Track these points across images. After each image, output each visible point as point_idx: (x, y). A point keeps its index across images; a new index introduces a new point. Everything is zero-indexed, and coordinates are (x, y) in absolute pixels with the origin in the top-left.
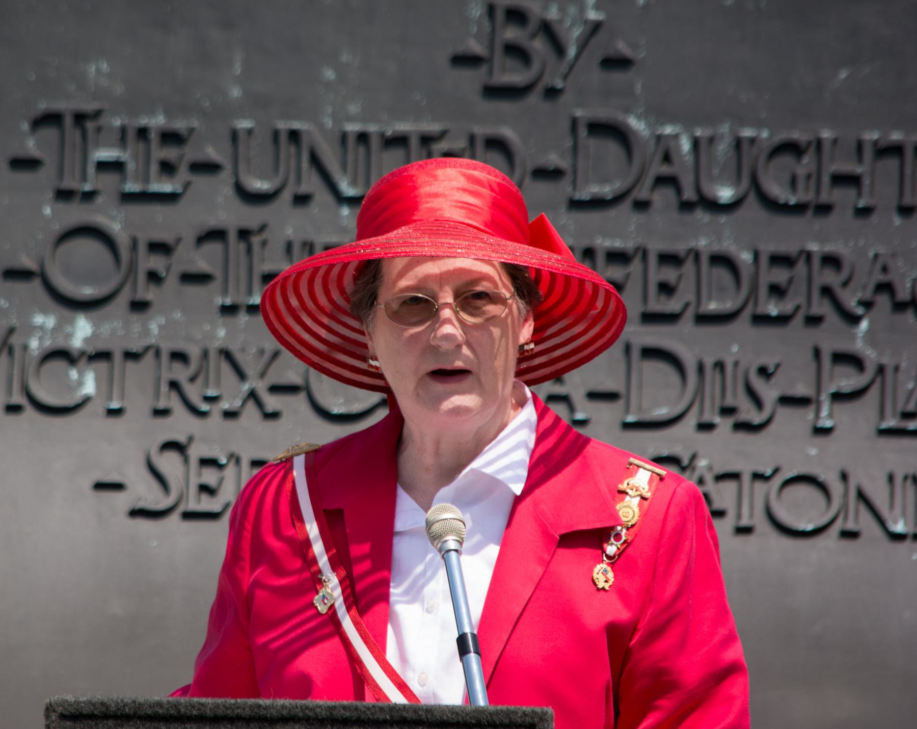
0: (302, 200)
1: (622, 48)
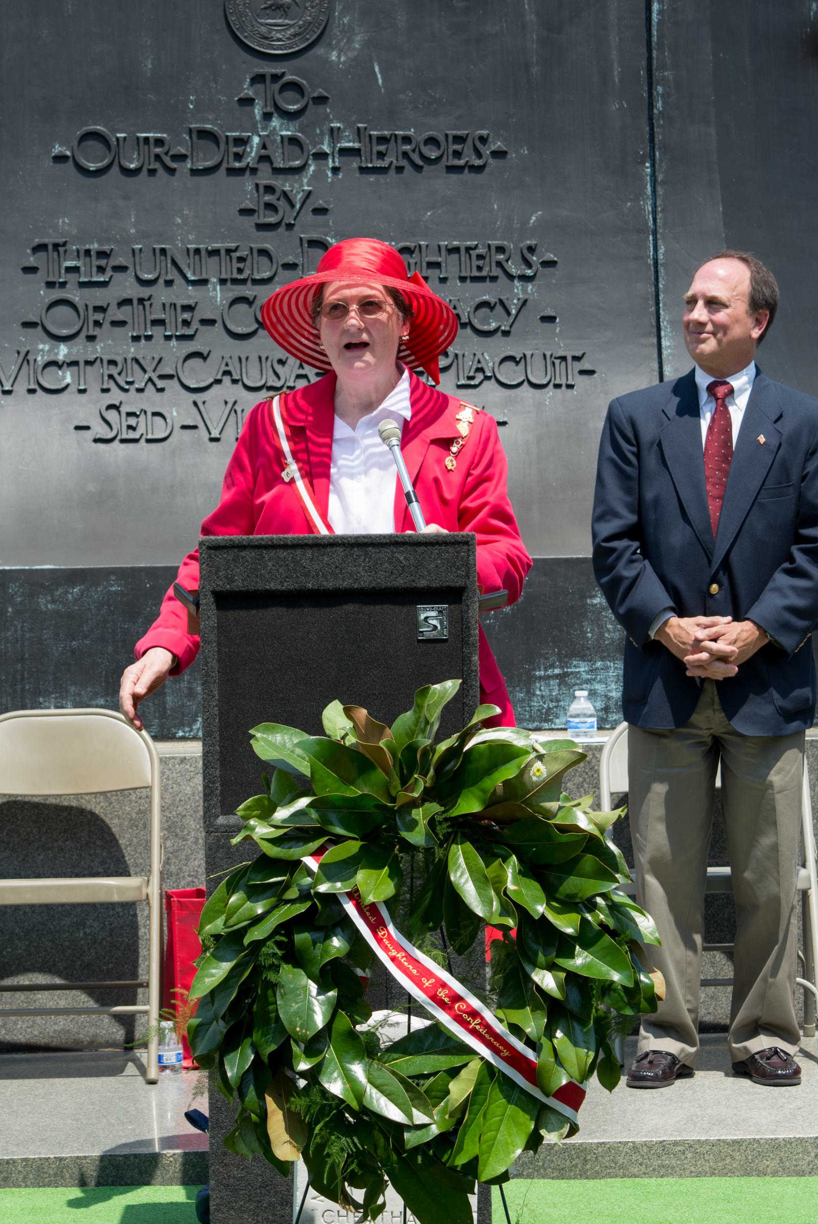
0: (169, 283)
1: (321, 203)
